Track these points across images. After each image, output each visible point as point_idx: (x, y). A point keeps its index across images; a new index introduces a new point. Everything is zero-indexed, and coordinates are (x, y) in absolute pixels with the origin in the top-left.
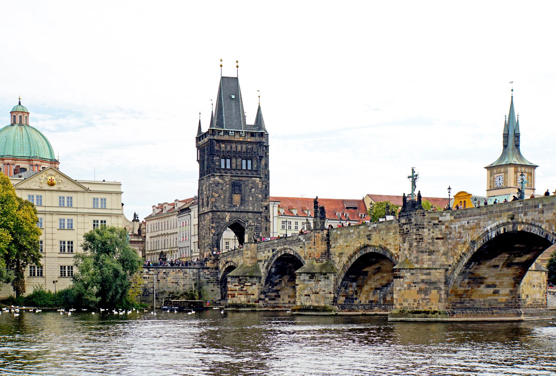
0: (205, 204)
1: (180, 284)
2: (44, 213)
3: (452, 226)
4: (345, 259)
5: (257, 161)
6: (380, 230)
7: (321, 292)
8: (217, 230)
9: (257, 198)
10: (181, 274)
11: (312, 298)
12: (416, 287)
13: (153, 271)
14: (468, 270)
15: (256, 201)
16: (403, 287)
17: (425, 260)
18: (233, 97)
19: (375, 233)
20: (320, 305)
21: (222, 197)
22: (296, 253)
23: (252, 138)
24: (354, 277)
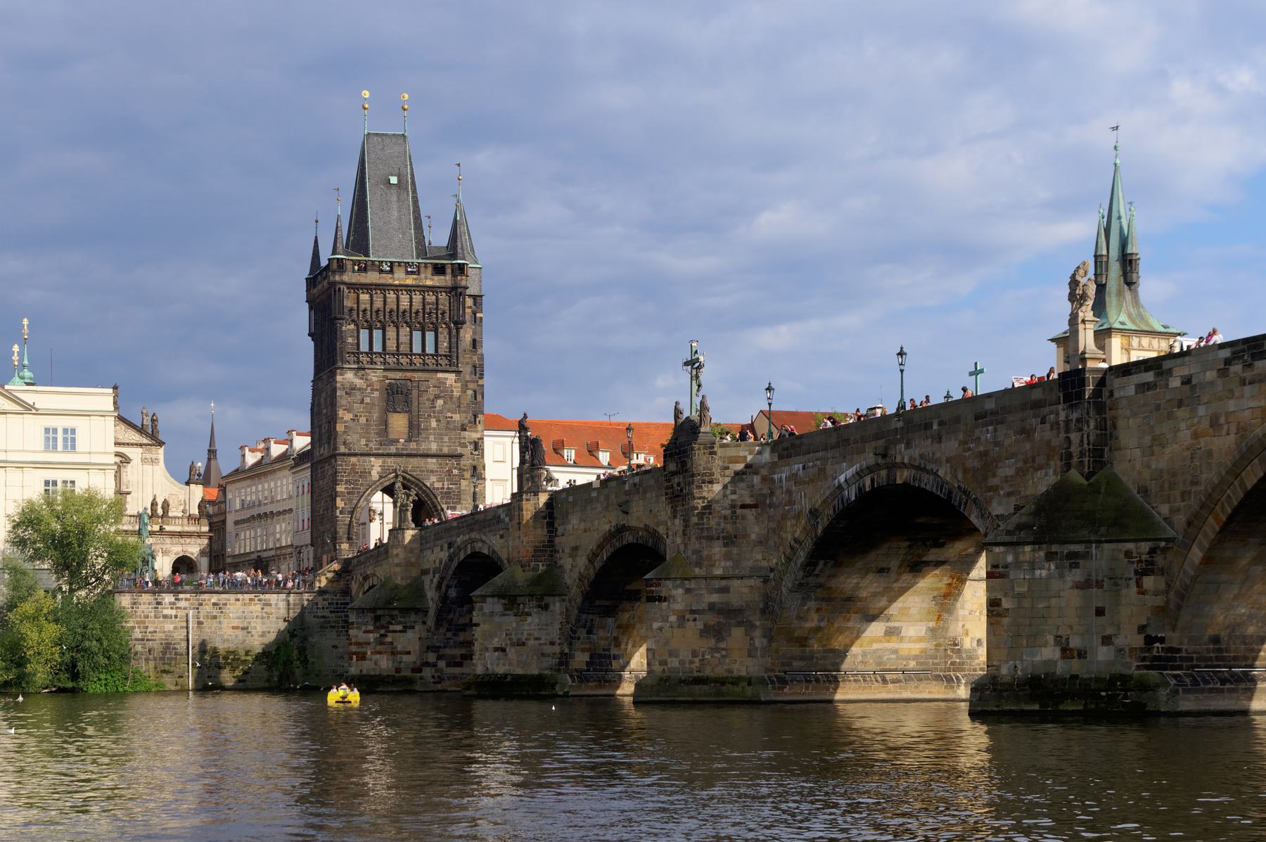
0: (325, 439)
1: (254, 632)
3: (776, 477)
4: (582, 561)
5: (450, 333)
6: (645, 492)
7: (531, 642)
8: (350, 500)
9: (448, 422)
10: (256, 608)
11: (510, 655)
12: (698, 623)
13: (186, 599)
14: (812, 580)
15: (447, 428)
16: (667, 621)
18: (394, 180)
19: (636, 497)
20: (529, 673)
21: (363, 420)
22: (494, 552)
23: (436, 278)
24: (607, 603)
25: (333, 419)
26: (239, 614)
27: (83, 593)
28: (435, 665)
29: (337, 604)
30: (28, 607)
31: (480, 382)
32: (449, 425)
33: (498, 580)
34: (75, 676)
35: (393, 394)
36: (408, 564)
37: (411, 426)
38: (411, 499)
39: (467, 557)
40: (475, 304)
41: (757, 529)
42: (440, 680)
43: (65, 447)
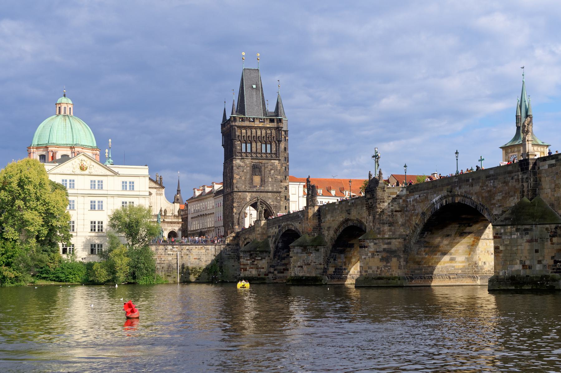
0: (228, 185)
2: (76, 195)
5: (276, 145)
8: (239, 209)
9: (276, 179)
10: (203, 251)
13: (177, 248)
14: (422, 239)
17: (386, 231)
21: (243, 178)
22: (297, 229)
23: (271, 124)
24: (341, 249)
25: (232, 178)
26: (197, 253)
27: (137, 245)
28: (273, 273)
29: (234, 249)
30: (117, 251)
31: (288, 164)
32: (276, 180)
33: (299, 240)
34: (134, 278)
35: (255, 168)
36: (263, 234)
37: (261, 181)
38: (263, 209)
39: (286, 231)
40: (285, 134)
41: (401, 220)
42: (275, 279)
43: (130, 189)
